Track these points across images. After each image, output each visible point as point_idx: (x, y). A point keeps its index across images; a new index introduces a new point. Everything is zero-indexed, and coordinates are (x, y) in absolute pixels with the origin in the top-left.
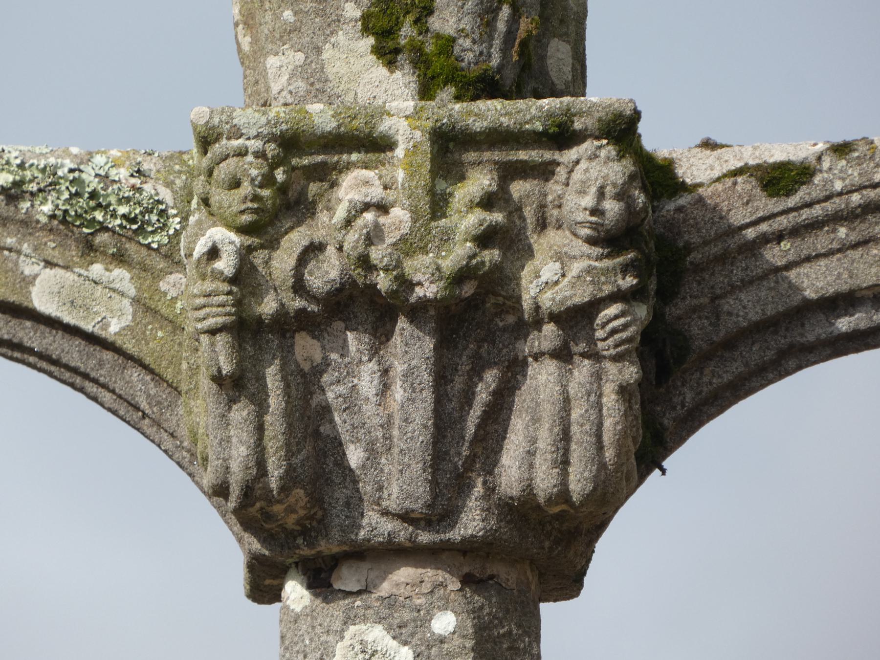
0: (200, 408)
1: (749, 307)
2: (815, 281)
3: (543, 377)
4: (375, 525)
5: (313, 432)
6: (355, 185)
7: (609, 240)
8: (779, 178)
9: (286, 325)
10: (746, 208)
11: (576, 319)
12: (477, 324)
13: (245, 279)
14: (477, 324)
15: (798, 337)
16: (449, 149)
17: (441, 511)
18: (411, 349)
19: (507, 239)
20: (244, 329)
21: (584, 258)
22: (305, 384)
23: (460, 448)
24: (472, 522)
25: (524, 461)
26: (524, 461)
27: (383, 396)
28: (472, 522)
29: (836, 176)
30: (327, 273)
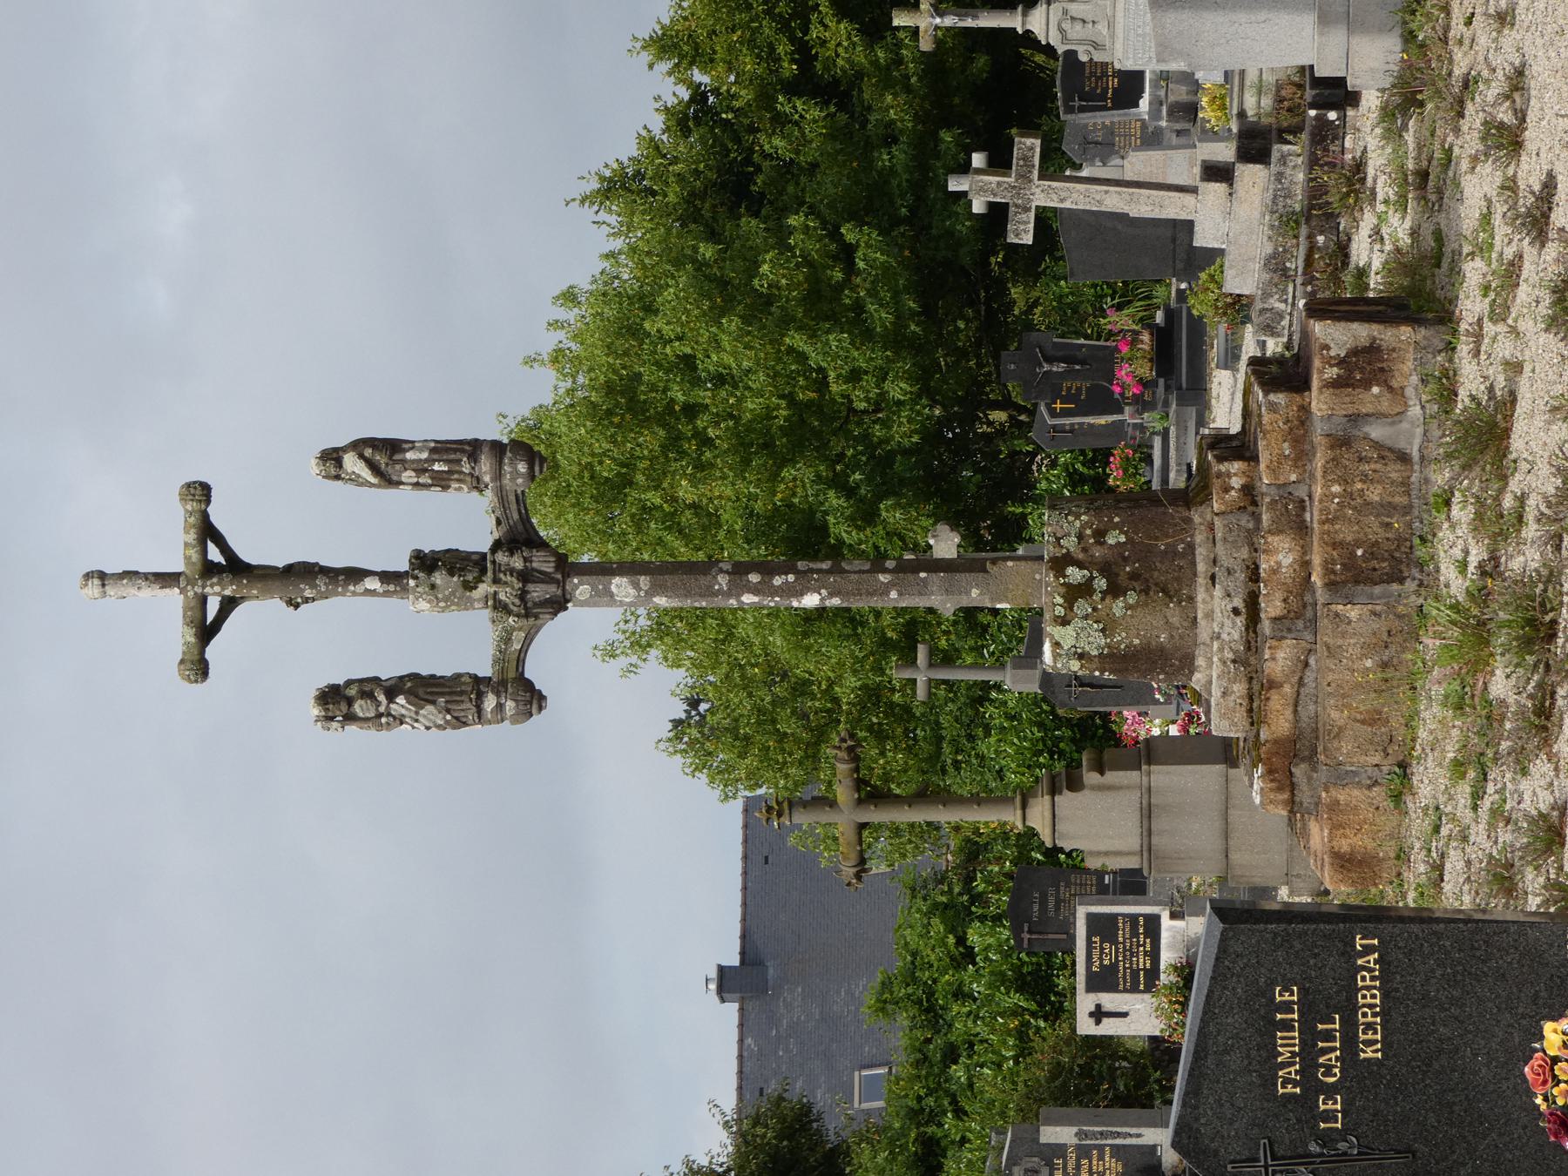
0: (539, 622)
1: (520, 528)
2: (516, 516)
3: (535, 565)
4: (559, 592)
5: (544, 603)
6: (502, 596)
7: (512, 554)
8: (499, 522)
9: (526, 608)
10: (504, 528)
11: (525, 560)
12: (526, 576)
13: (518, 616)
14: (526, 576)
15: (525, 520)
16: (496, 581)
17: (557, 582)
18: (530, 587)
19: (512, 571)
20: (527, 616)
21: (515, 558)
22: (536, 605)
23: (546, 578)
24: (559, 576)
25: (549, 568)
26: (549, 568)
27: (538, 592)
28: (559, 576)
29: (498, 513)
30: (517, 601)
